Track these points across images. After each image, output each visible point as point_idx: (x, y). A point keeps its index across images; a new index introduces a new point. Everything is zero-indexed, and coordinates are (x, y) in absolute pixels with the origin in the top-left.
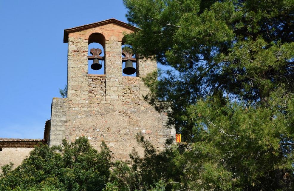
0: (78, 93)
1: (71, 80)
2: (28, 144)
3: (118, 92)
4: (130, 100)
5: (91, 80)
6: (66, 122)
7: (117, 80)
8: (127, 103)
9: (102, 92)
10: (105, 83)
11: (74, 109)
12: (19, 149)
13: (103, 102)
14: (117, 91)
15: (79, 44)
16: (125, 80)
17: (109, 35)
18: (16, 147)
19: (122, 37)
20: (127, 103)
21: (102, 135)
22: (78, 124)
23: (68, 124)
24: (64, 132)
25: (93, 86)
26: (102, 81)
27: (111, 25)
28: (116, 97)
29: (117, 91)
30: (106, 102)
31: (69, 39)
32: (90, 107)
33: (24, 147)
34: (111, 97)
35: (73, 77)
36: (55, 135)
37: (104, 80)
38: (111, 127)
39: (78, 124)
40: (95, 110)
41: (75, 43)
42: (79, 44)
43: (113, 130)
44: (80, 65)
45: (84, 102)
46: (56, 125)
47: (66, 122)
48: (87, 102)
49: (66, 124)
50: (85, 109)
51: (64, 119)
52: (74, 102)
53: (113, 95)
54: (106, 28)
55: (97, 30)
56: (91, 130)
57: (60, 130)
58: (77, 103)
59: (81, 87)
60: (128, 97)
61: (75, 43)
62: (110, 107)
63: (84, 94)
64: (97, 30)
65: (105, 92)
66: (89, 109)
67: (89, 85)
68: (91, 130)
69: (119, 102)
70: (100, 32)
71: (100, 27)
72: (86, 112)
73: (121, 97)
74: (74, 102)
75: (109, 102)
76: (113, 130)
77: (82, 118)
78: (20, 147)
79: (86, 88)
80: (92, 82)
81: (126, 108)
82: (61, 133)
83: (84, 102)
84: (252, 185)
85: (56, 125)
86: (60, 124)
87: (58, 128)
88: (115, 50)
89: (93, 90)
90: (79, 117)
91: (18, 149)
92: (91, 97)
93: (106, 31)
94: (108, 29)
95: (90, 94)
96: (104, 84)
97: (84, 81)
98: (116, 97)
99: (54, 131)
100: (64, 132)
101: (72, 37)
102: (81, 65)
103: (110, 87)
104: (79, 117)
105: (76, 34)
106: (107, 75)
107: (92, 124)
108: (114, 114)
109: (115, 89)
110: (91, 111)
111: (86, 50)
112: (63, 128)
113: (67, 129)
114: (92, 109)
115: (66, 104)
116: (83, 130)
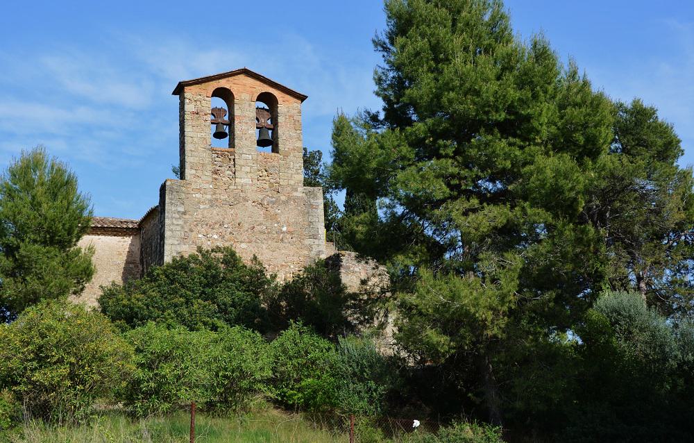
0: (199, 173)
1: (190, 155)
2: (115, 231)
3: (251, 175)
4: (267, 186)
5: (216, 155)
6: (184, 213)
7: (250, 156)
8: (262, 190)
9: (231, 173)
10: (234, 160)
11: (194, 195)
12: (102, 237)
13: (232, 187)
14: (250, 172)
15: (198, 103)
16: (260, 158)
17: (239, 91)
18: (99, 235)
19: (504, 5)
20: (262, 190)
21: (231, 233)
22: (200, 216)
23: (187, 216)
24: (183, 228)
25: (219, 164)
26: (231, 157)
27: (242, 77)
28: (248, 181)
29: (250, 172)
30: (235, 188)
31: (185, 95)
32: (215, 194)
33: (109, 235)
34: (243, 181)
35: (192, 151)
36: (172, 231)
37: (233, 157)
38: (243, 222)
39: (200, 216)
40: (222, 197)
41: (193, 101)
42: (198, 103)
43: (246, 226)
44: (200, 134)
45: (207, 186)
46: (172, 218)
47: (184, 213)
48: (211, 186)
49: (184, 216)
50: (209, 197)
51: (181, 209)
52: (193, 186)
53: (245, 179)
54: (236, 81)
55: (223, 83)
56: (217, 226)
57: (177, 225)
58: (198, 188)
59: (203, 165)
60: (264, 181)
61: (193, 101)
62: (242, 195)
63: (207, 175)
64: (223, 83)
65: (234, 173)
66: (214, 197)
67: (213, 162)
68: (217, 226)
69: (253, 188)
70: (227, 86)
71: (227, 79)
72: (211, 201)
73: (255, 181)
74: (193, 186)
75: (239, 187)
76: (246, 226)
77: (204, 209)
78: (104, 234)
79: (210, 167)
80: (217, 159)
81: (261, 197)
82: (179, 228)
83: (207, 186)
84: (576, 347)
85: (172, 218)
86: (177, 216)
87: (175, 222)
88: (247, 113)
89: (218, 170)
90: (202, 207)
91: (100, 237)
92: (216, 179)
93: (234, 85)
94: (236, 81)
95: (215, 176)
96: (232, 163)
97: (207, 157)
98: (248, 181)
99: (169, 225)
100: (183, 228)
101: (189, 92)
102: (202, 134)
103: (241, 166)
104: (202, 207)
105: (195, 88)
106: (236, 149)
107: (218, 217)
108: (247, 204)
109: (248, 169)
110: (217, 200)
111: (208, 112)
112: (180, 222)
113: (185, 223)
114: (218, 196)
115: (184, 189)
116: (207, 225)
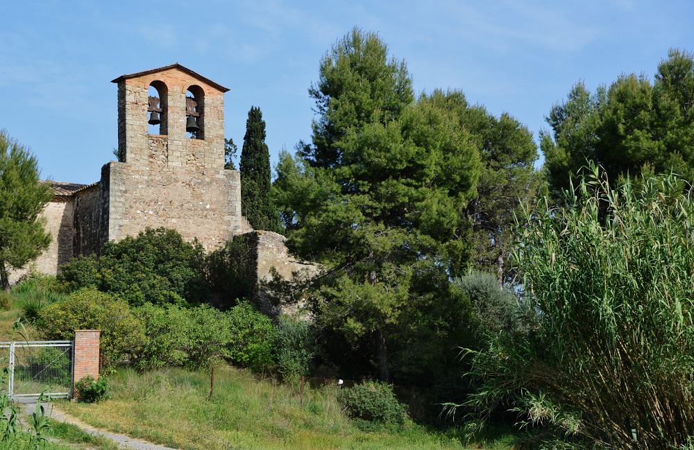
4: (194, 169)
5: (152, 141)
6: (125, 192)
8: (190, 172)
10: (167, 145)
13: (165, 170)
14: (181, 157)
20: (190, 172)
21: (164, 210)
22: (139, 195)
24: (124, 204)
27: (174, 71)
29: (181, 157)
32: (151, 175)
34: (174, 164)
36: (115, 207)
39: (139, 195)
40: (157, 179)
47: (125, 192)
48: (148, 169)
50: (146, 178)
53: (175, 163)
56: (152, 203)
62: (174, 176)
63: (145, 159)
64: (158, 77)
65: (167, 157)
66: (150, 178)
68: (152, 203)
70: (162, 80)
72: (147, 181)
74: (133, 168)
75: (171, 170)
79: (147, 152)
80: (153, 145)
81: (189, 178)
82: (121, 205)
83: (144, 168)
86: (120, 194)
87: (118, 200)
88: (178, 104)
90: (140, 186)
92: (152, 162)
93: (169, 78)
95: (152, 160)
96: (165, 148)
97: (144, 142)
99: (113, 202)
104: (140, 186)
112: (122, 200)
113: (126, 200)
115: (125, 171)
116: (144, 202)
